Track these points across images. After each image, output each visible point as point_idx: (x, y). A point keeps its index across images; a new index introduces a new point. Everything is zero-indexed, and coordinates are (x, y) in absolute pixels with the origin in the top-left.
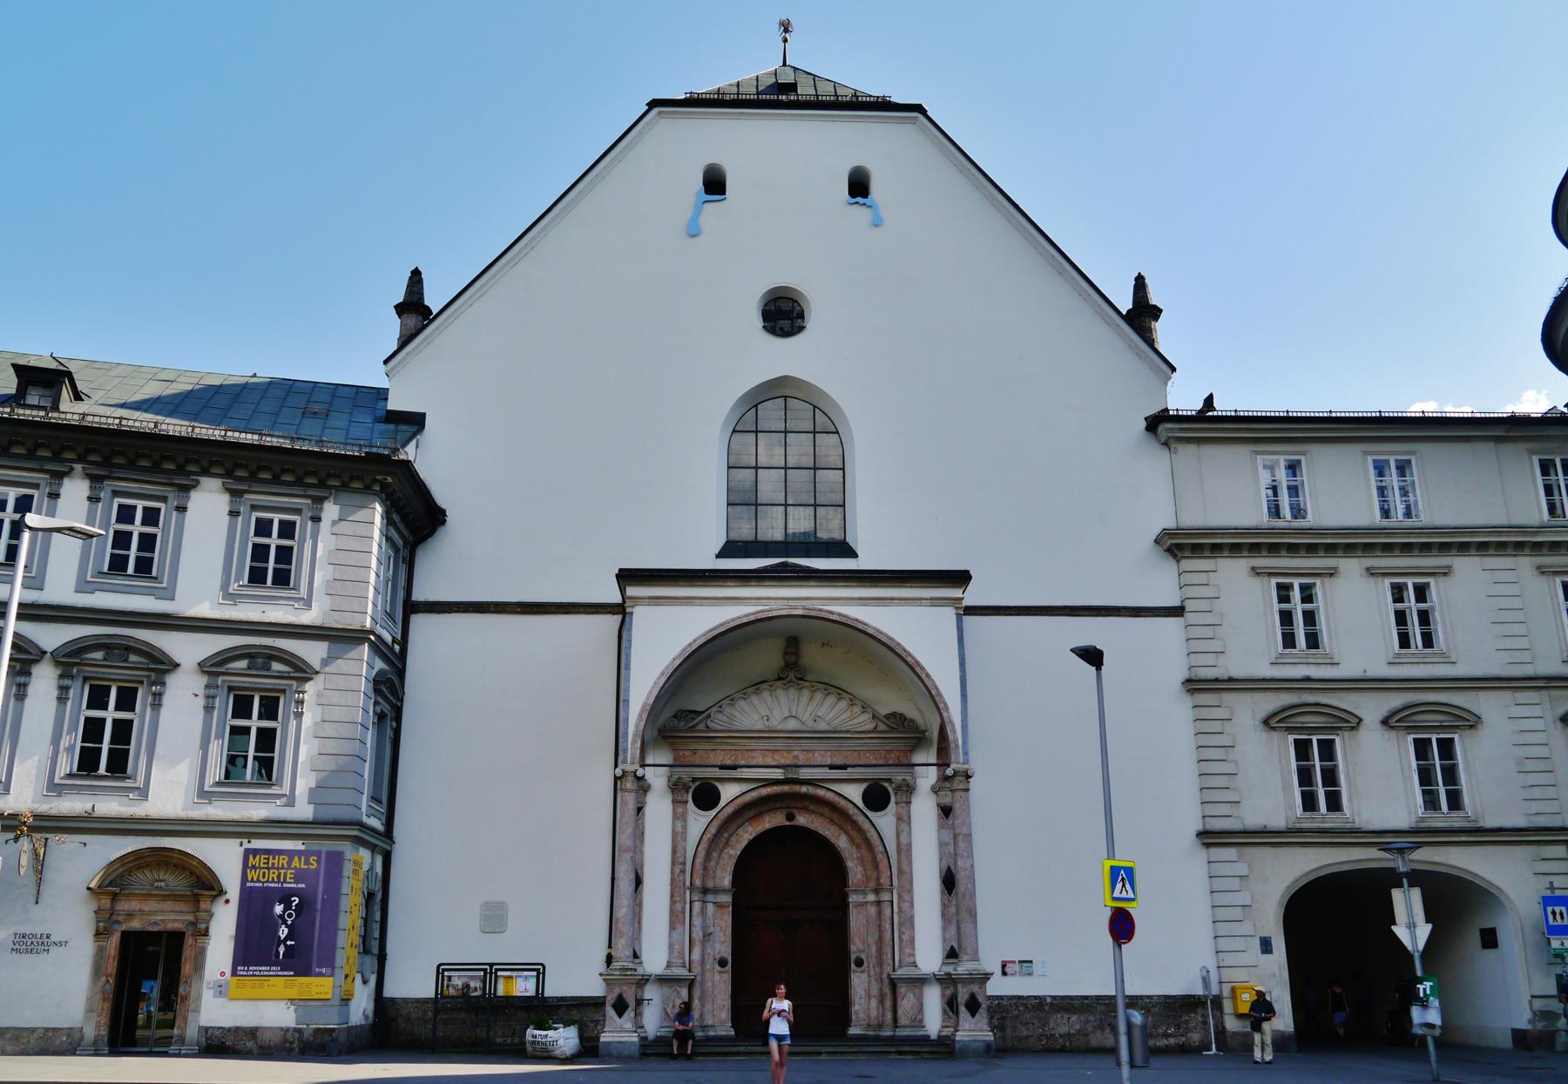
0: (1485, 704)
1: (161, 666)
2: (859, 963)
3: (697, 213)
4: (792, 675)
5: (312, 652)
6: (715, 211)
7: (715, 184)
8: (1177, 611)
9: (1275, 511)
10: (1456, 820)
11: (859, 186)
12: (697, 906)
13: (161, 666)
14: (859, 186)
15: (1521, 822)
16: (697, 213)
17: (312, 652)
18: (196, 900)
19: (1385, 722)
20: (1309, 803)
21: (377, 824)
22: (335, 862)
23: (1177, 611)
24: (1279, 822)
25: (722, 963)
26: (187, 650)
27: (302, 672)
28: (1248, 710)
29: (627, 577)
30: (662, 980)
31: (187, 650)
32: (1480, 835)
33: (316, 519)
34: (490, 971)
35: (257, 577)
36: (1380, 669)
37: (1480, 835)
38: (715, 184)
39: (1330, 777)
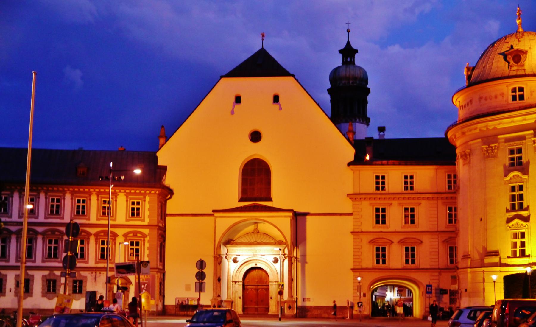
0: (426, 239)
1: (115, 235)
2: (271, 298)
3: (234, 107)
4: (255, 231)
5: (146, 231)
6: (237, 106)
7: (238, 100)
8: (351, 214)
9: (377, 189)
10: (413, 266)
11: (276, 99)
12: (234, 285)
13: (115, 235)
14: (276, 99)
15: (428, 267)
16: (234, 107)
17: (146, 231)
18: (126, 284)
19: (399, 242)
20: (378, 262)
21: (161, 267)
22: (153, 277)
23: (351, 214)
24: (370, 266)
25: (240, 298)
26: (120, 232)
27: (144, 236)
28: (365, 239)
29: (214, 211)
30: (225, 301)
31: (120, 232)
32: (418, 269)
33: (145, 201)
34: (187, 299)
35: (133, 215)
36: (399, 229)
37: (418, 269)
38: (238, 100)
39: (384, 256)
